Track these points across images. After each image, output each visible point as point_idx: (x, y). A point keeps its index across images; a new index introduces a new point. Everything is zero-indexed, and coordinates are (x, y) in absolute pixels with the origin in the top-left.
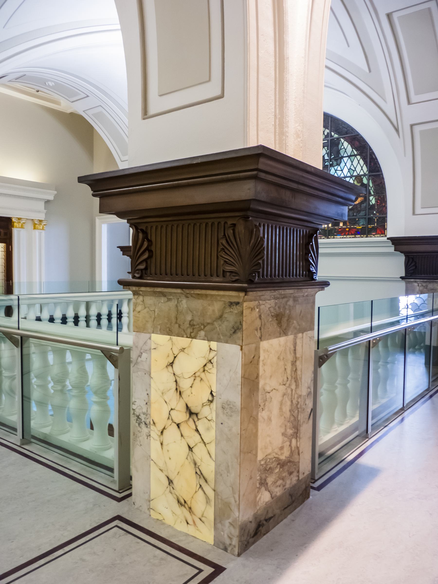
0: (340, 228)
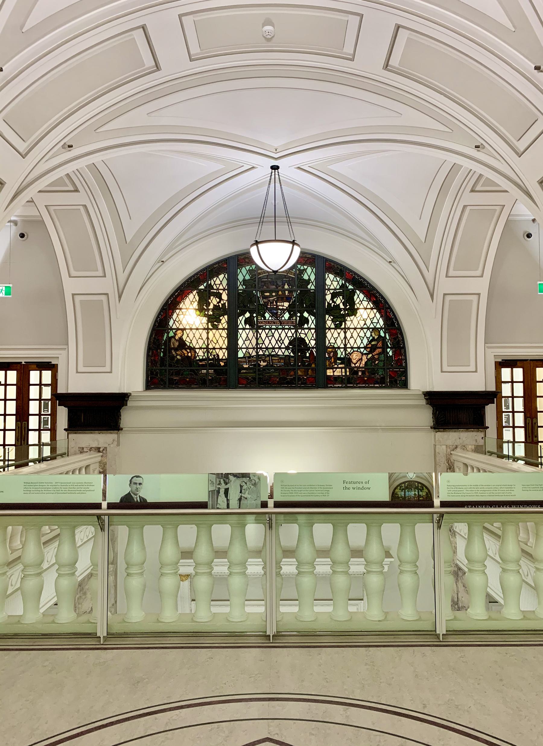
0: (359, 377)
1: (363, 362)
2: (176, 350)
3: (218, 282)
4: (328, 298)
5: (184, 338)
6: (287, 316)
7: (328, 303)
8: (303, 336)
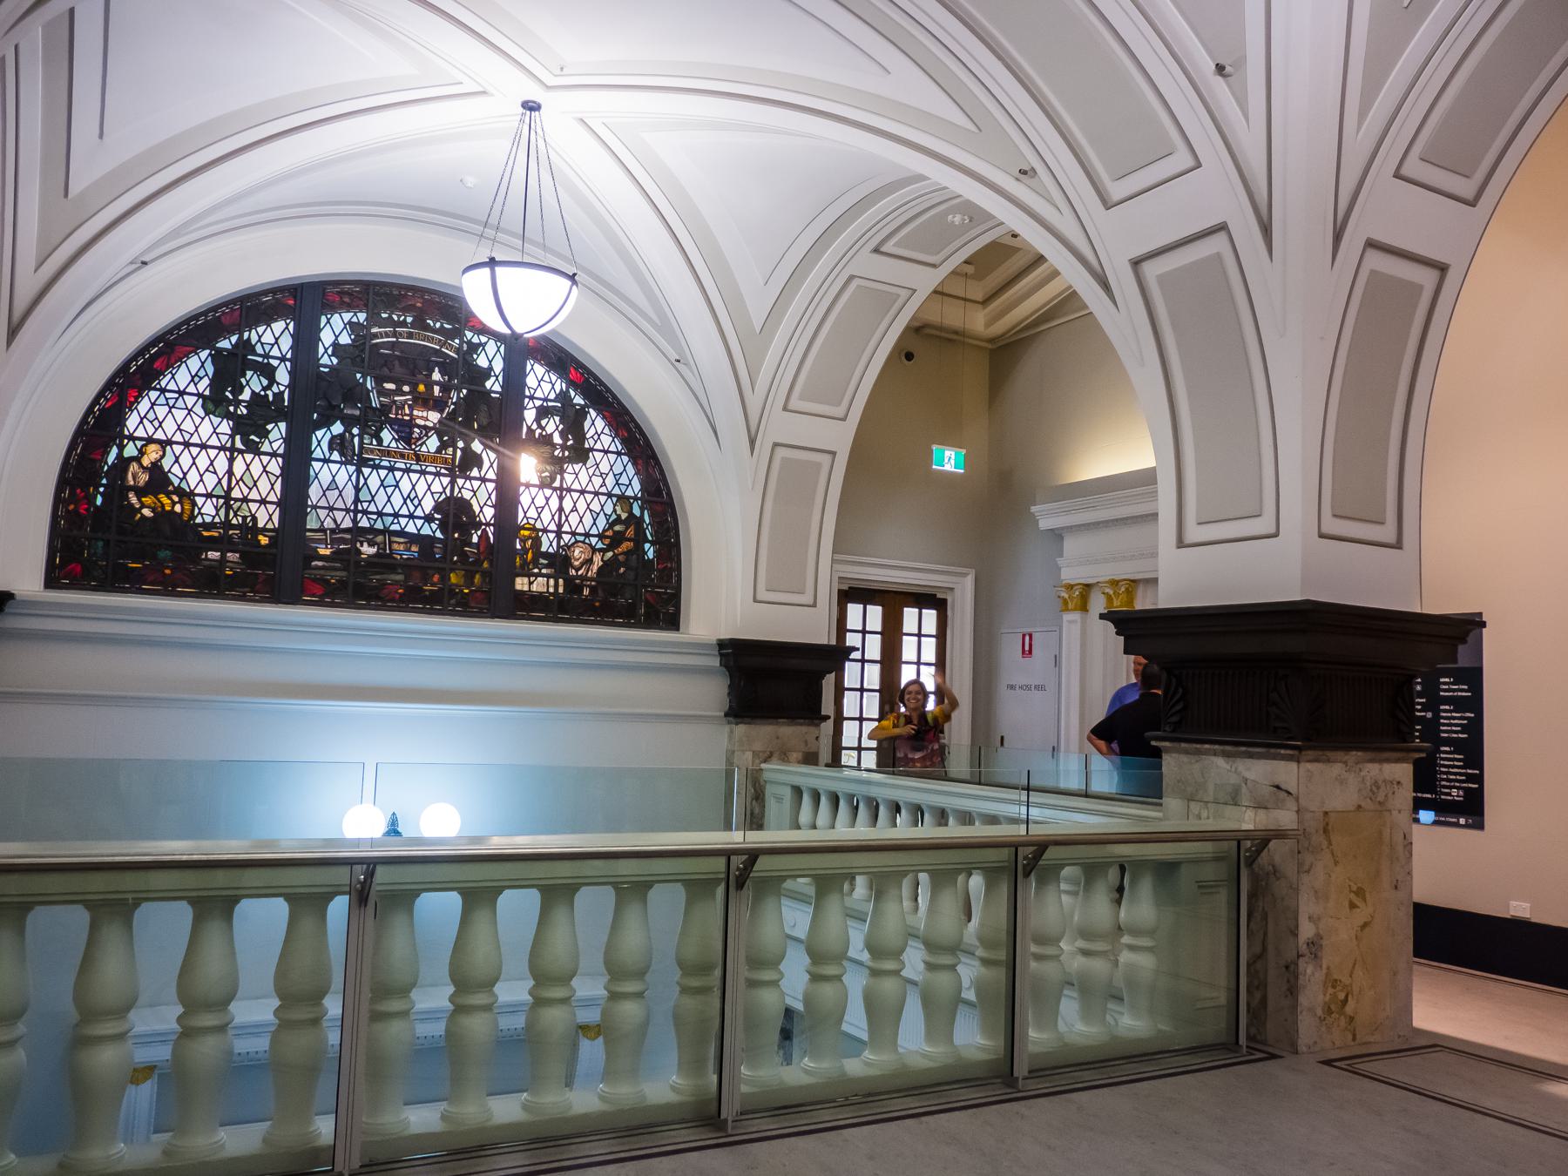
1: (595, 568)
2: (140, 492)
3: (268, 338)
4: (530, 415)
5: (166, 464)
6: (433, 443)
7: (529, 428)
8: (467, 495)
